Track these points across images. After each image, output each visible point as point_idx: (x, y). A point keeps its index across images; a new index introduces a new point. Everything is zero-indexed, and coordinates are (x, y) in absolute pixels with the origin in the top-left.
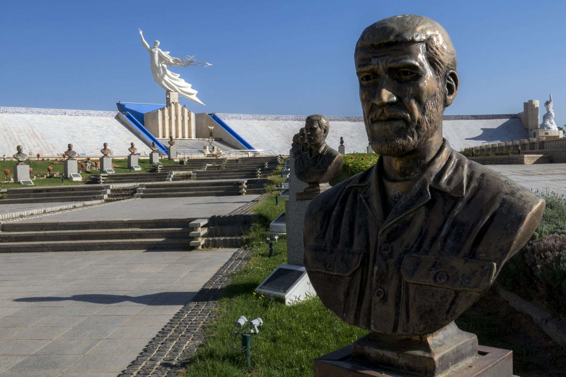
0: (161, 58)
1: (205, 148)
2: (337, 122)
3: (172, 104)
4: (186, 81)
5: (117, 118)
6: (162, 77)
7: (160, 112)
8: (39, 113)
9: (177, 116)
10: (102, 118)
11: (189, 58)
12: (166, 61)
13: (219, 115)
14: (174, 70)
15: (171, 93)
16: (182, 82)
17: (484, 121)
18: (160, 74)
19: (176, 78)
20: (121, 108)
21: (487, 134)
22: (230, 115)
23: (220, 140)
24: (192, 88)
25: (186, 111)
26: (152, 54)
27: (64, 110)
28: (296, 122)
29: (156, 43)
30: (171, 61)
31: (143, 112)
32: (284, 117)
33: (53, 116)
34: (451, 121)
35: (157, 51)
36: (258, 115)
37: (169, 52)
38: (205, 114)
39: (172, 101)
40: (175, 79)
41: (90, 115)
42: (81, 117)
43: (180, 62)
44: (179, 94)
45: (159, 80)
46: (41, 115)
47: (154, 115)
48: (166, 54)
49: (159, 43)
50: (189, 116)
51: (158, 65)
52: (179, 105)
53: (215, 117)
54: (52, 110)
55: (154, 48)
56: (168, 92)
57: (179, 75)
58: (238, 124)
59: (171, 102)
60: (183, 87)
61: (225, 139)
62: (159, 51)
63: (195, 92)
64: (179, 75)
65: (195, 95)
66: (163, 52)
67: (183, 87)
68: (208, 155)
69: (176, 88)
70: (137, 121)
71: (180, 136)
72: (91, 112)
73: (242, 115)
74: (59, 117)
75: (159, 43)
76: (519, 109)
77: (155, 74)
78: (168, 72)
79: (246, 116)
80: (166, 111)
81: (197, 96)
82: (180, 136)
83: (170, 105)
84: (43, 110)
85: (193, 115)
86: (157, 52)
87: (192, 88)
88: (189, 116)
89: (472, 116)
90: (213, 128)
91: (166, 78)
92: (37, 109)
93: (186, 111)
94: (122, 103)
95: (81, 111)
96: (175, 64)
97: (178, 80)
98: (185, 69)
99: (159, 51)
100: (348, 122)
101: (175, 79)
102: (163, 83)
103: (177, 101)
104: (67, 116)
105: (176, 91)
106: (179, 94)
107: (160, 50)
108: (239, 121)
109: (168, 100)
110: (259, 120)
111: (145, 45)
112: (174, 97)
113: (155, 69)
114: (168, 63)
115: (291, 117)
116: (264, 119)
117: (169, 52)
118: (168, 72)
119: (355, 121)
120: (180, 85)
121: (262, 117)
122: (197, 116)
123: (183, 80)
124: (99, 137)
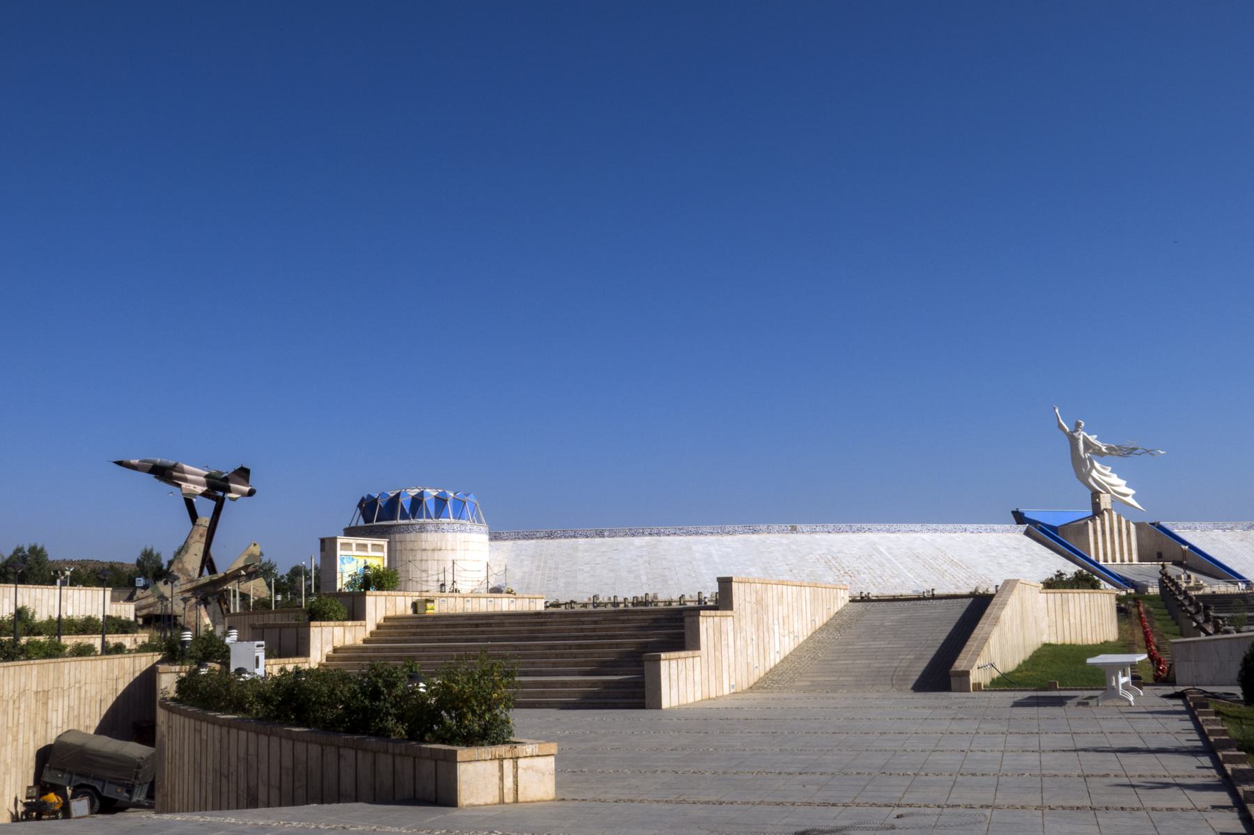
0: (1088, 445)
5: (1027, 533)
6: (1090, 471)
7: (1090, 524)
8: (936, 530)
13: (1167, 524)
14: (1103, 464)
16: (1114, 479)
19: (1107, 472)
20: (1019, 518)
26: (1073, 441)
29: (1078, 425)
30: (1104, 449)
31: (1056, 525)
33: (952, 535)
35: (1081, 435)
39: (1103, 507)
41: (994, 530)
42: (984, 534)
44: (1112, 496)
47: (1079, 528)
54: (951, 526)
55: (1076, 431)
56: (1095, 495)
63: (1131, 492)
72: (996, 527)
74: (958, 534)
77: (1080, 468)
78: (1097, 465)
80: (1098, 522)
81: (1134, 497)
85: (1133, 527)
87: (1127, 486)
91: (1094, 473)
102: (1091, 480)
104: (968, 535)
105: (1108, 492)
106: (1112, 496)
112: (1105, 501)
114: (1098, 453)
122: (1139, 526)
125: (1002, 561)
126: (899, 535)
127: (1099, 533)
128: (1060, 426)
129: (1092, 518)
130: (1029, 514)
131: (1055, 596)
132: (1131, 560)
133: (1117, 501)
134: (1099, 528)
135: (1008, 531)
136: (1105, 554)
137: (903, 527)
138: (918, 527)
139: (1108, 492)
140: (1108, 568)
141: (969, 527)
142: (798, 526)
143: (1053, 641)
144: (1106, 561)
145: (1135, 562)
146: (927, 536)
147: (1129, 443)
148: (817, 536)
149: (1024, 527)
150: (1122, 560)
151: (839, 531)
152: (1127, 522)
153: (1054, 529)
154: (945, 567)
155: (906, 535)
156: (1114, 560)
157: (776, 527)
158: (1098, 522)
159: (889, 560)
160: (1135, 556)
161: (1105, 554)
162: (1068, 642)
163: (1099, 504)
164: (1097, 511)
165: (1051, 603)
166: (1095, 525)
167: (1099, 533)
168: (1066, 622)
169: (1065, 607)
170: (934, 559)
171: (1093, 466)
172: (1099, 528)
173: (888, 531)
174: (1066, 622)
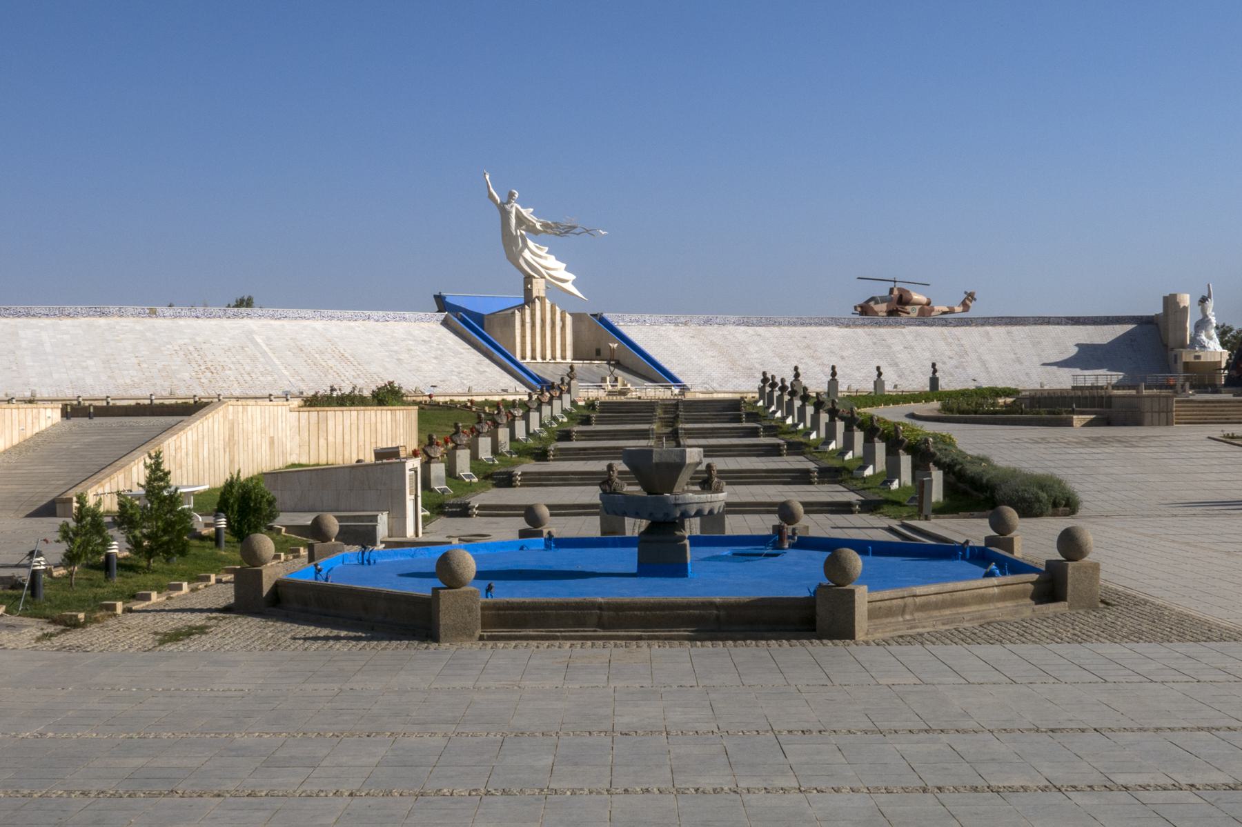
0: (521, 220)
1: (604, 380)
2: (814, 329)
4: (557, 259)
5: (445, 323)
8: (332, 318)
10: (422, 324)
13: (610, 317)
14: (541, 243)
17: (1090, 328)
19: (543, 253)
20: (442, 304)
21: (1087, 356)
22: (627, 317)
23: (619, 365)
24: (566, 269)
26: (505, 214)
27: (367, 313)
28: (742, 328)
29: (511, 195)
30: (538, 226)
32: (720, 319)
33: (352, 323)
34: (1027, 328)
35: (514, 208)
40: (540, 257)
42: (392, 323)
43: (551, 228)
44: (547, 282)
46: (334, 322)
47: (505, 319)
48: (527, 213)
50: (563, 320)
53: (602, 320)
54: (350, 313)
55: (509, 202)
56: (528, 279)
58: (645, 333)
61: (628, 362)
63: (571, 277)
68: (610, 393)
70: (478, 328)
71: (549, 356)
72: (407, 314)
73: (647, 316)
74: (359, 323)
76: (1156, 309)
77: (512, 249)
78: (530, 243)
79: (655, 317)
80: (528, 312)
81: (574, 283)
82: (549, 356)
83: (534, 302)
84: (338, 313)
85: (569, 319)
86: (514, 211)
87: (566, 269)
88: (563, 320)
89: (1068, 318)
90: (601, 341)
91: (527, 254)
92: (330, 312)
95: (392, 313)
97: (546, 258)
100: (836, 329)
101: (540, 257)
102: (521, 261)
103: (542, 294)
104: (372, 323)
105: (543, 277)
106: (547, 282)
108: (644, 329)
109: (528, 292)
110: (677, 324)
112: (538, 288)
114: (532, 230)
115: (733, 318)
116: (686, 324)
119: (848, 326)
120: (548, 264)
122: (577, 318)
123: (552, 258)
125: (404, 356)
126: (285, 322)
127: (528, 326)
128: (491, 196)
129: (521, 308)
130: (452, 298)
131: (313, 414)
132: (554, 358)
133: (554, 289)
134: (528, 319)
135: (422, 320)
136: (533, 350)
137: (290, 312)
138: (310, 313)
139: (543, 277)
140: (529, 368)
141: (374, 314)
142: (159, 309)
143: (304, 461)
144: (523, 358)
145: (569, 360)
146: (319, 325)
147: (566, 221)
148: (182, 322)
149: (442, 316)
150: (554, 358)
151: (210, 316)
152: (563, 313)
153: (479, 318)
154: (331, 363)
155: (294, 323)
156: (543, 358)
157: (130, 309)
158: (528, 312)
159: (264, 354)
160: (569, 353)
161: (533, 350)
162: (323, 461)
163: (531, 290)
164: (529, 300)
165: (304, 422)
166: (523, 315)
167: (528, 326)
168: (322, 441)
169: (322, 426)
170: (321, 353)
171: (525, 245)
172: (528, 319)
173: (272, 317)
174: (322, 441)
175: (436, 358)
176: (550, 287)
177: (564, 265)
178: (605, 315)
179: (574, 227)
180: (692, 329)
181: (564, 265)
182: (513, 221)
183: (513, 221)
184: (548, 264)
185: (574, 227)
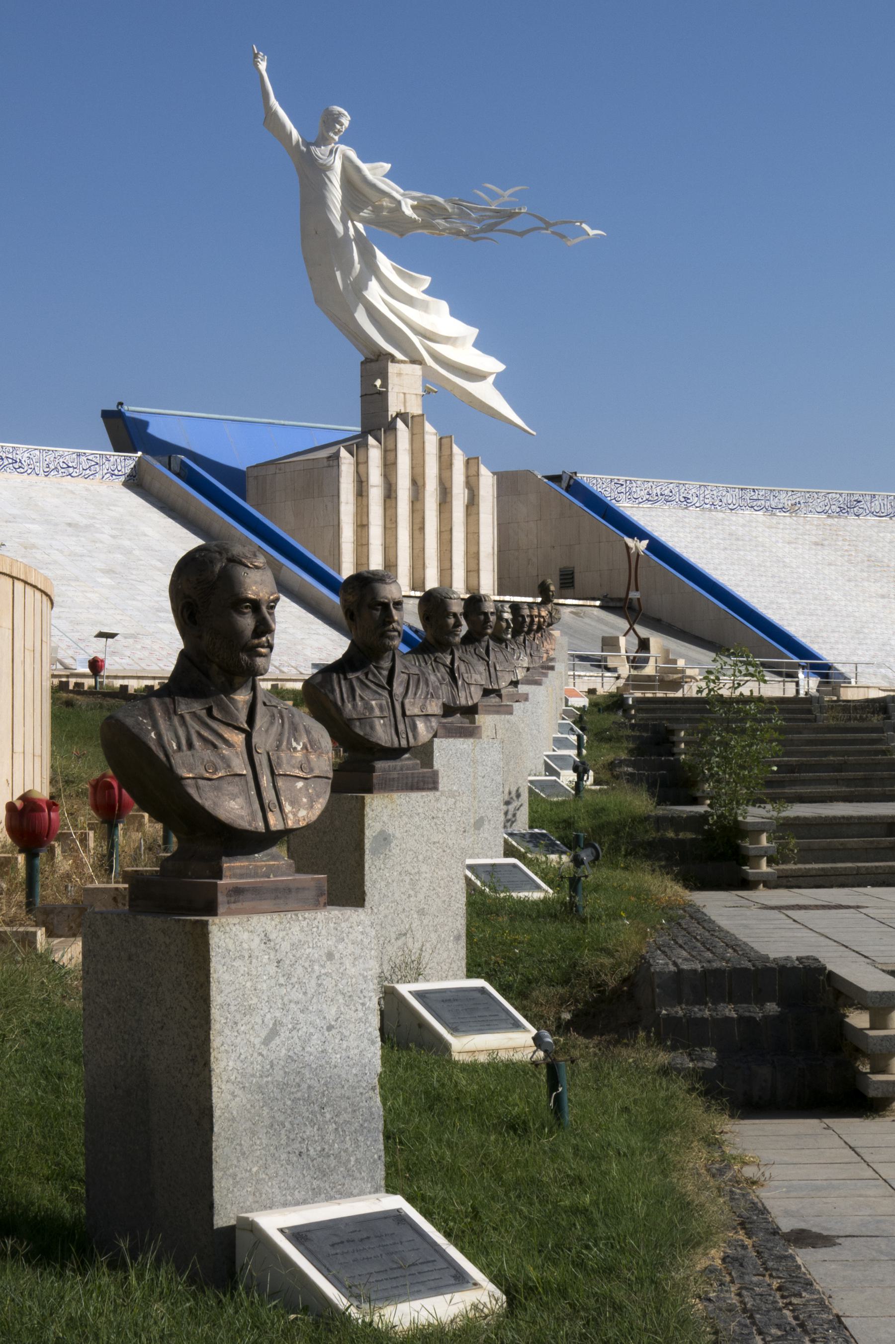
0: (357, 192)
3: (400, 424)
4: (454, 313)
5: (136, 482)
6: (358, 289)
7: (347, 461)
9: (417, 485)
11: (494, 196)
12: (377, 209)
13: (598, 482)
14: (408, 262)
15: (392, 368)
16: (439, 318)
18: (346, 273)
19: (415, 292)
20: (124, 431)
22: (641, 486)
24: (477, 344)
25: (459, 458)
26: (312, 174)
29: (331, 120)
30: (408, 211)
31: (240, 460)
35: (337, 157)
36: (762, 490)
37: (387, 166)
38: (529, 474)
39: (394, 406)
40: (409, 301)
43: (447, 217)
44: (428, 376)
45: (338, 305)
47: (312, 476)
48: (376, 172)
49: (346, 121)
51: (340, 228)
52: (428, 428)
53: (577, 489)
55: (323, 141)
56: (375, 364)
57: (426, 281)
59: (392, 411)
60: (447, 340)
62: (346, 159)
63: (492, 365)
64: (426, 281)
65: (491, 379)
66: (365, 168)
67: (447, 340)
69: (415, 339)
73: (692, 488)
75: (346, 121)
77: (325, 271)
78: (384, 263)
79: (714, 490)
80: (375, 454)
81: (500, 383)
83: (391, 427)
87: (477, 344)
91: (374, 292)
93: (459, 458)
94: (131, 409)
96: (425, 225)
97: (424, 307)
98: (462, 250)
99: (346, 158)
101: (409, 301)
102: (361, 316)
103: (415, 408)
105: (416, 360)
107: (352, 154)
110: (771, 510)
111: (283, 126)
112: (404, 389)
113: (320, 249)
116: (793, 509)
117: (387, 166)
118: (384, 263)
121: (785, 499)
122: (510, 485)
123: (443, 306)
124: (106, 580)
127: (376, 494)
129: (357, 445)
133: (446, 400)
139: (416, 360)
149: (127, 462)
153: (236, 478)
158: (375, 454)
163: (382, 396)
164: (376, 420)
167: (376, 494)
171: (371, 268)
175: (109, 572)
176: (432, 390)
177: (472, 333)
178: (584, 477)
179: (511, 215)
180: (812, 523)
181: (472, 333)
182: (335, 194)
183: (335, 194)
184: (426, 321)
185: (511, 215)
